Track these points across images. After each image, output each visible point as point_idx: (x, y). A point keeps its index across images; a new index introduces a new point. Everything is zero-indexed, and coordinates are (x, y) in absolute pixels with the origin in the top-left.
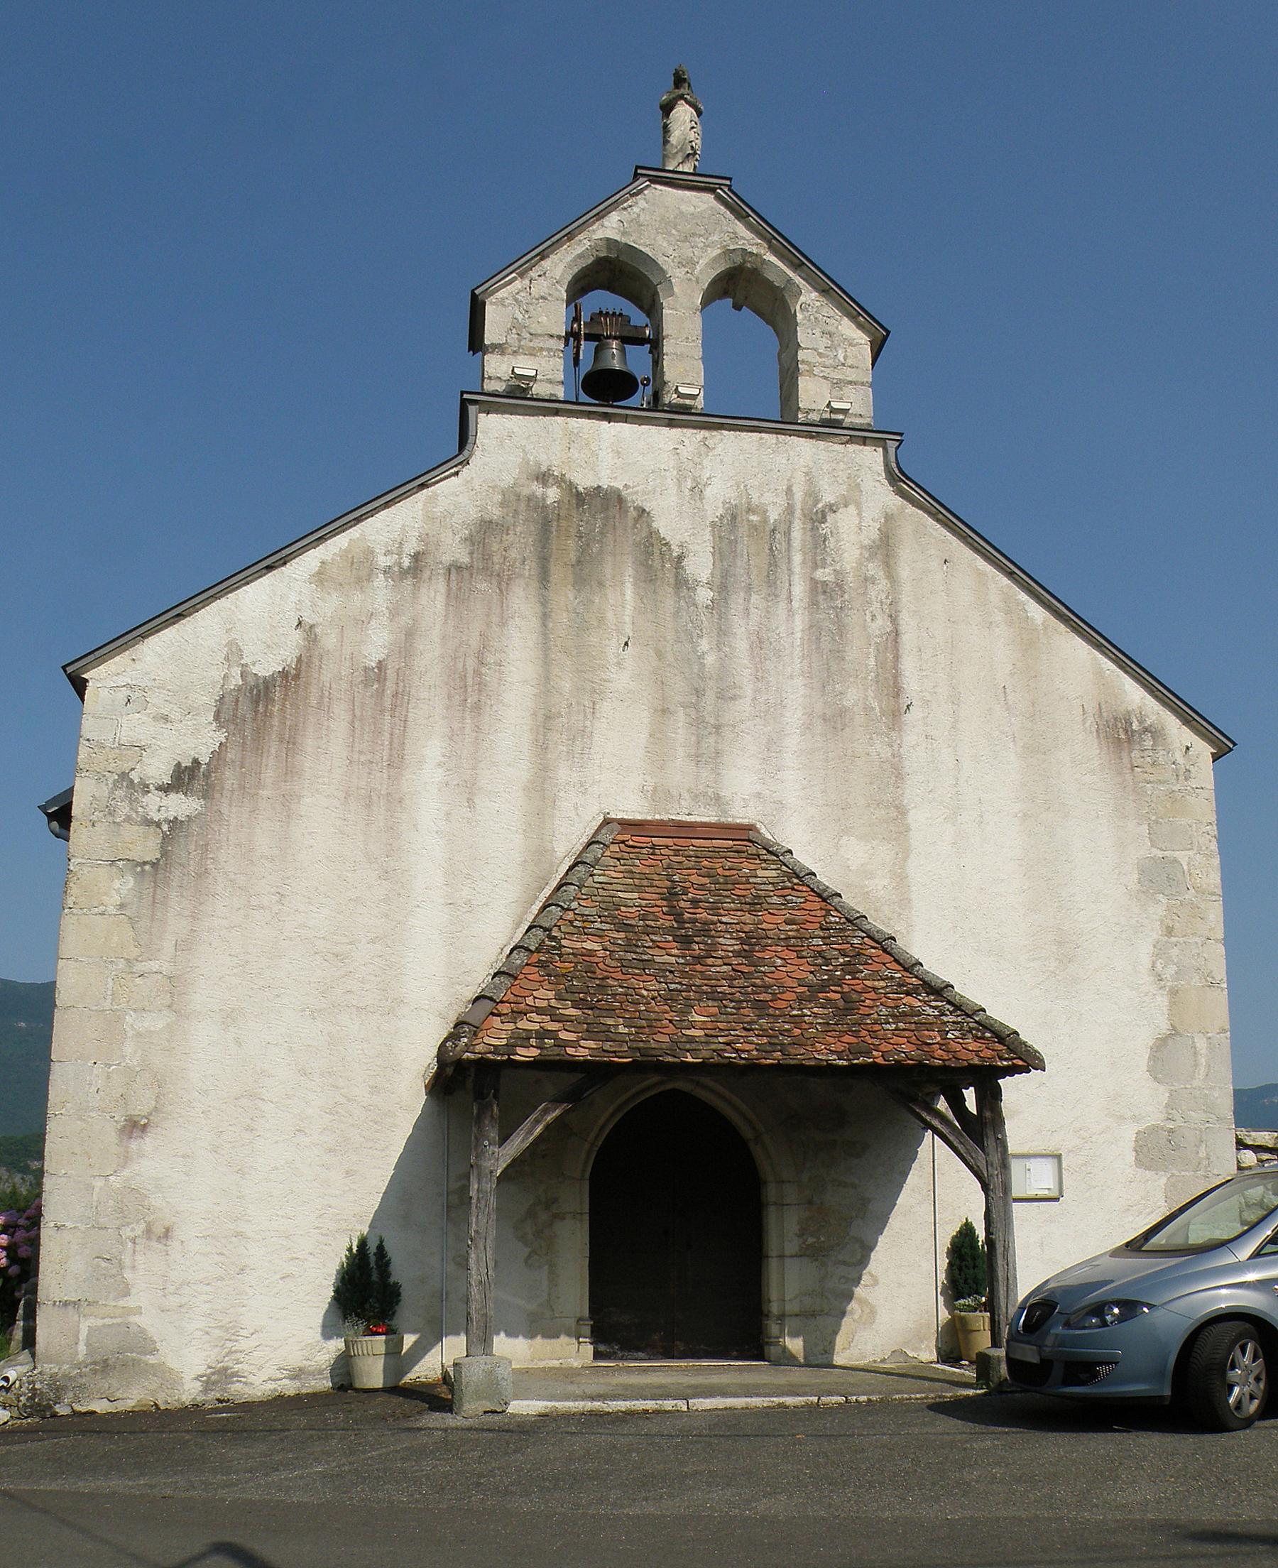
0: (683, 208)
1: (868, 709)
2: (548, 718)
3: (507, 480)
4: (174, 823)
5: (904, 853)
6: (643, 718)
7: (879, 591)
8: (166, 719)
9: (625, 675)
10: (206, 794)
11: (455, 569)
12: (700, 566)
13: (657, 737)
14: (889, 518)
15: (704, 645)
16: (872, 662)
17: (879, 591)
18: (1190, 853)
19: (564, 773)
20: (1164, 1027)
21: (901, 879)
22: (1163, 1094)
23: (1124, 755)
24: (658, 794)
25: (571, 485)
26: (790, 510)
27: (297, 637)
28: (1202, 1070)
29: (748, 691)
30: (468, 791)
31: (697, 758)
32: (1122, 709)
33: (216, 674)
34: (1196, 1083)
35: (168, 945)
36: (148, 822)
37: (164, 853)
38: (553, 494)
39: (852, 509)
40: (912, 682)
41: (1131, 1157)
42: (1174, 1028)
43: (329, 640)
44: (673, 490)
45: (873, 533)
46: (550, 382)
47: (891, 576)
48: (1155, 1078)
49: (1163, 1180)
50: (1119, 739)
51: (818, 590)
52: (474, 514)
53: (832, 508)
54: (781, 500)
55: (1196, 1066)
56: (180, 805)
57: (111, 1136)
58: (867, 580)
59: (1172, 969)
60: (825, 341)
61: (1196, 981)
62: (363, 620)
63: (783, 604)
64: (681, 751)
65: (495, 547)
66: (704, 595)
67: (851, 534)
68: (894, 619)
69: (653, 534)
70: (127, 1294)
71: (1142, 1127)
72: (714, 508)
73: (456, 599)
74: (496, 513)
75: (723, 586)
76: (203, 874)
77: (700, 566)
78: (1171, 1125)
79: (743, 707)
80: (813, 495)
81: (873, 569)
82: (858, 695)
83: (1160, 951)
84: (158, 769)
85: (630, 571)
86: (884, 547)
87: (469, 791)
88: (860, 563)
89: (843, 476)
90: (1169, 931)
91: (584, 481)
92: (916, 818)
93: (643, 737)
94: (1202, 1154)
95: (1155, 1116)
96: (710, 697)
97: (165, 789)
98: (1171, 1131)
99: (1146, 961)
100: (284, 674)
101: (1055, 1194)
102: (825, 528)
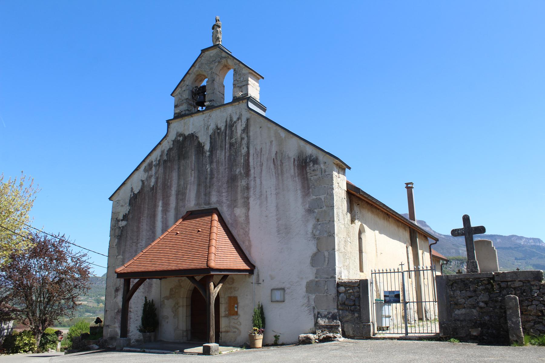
0: (211, 55)
1: (241, 174)
2: (179, 192)
3: (173, 138)
4: (123, 227)
5: (249, 209)
6: (195, 187)
7: (245, 142)
8: (122, 206)
9: (192, 177)
10: (127, 220)
11: (165, 161)
12: (207, 147)
13: (198, 192)
14: (248, 120)
15: (208, 166)
16: (242, 161)
17: (245, 142)
18: (325, 195)
19: (181, 204)
20: (314, 250)
21: (247, 217)
22: (314, 270)
23: (304, 170)
24: (198, 204)
25: (185, 135)
26: (226, 126)
27: (141, 184)
28: (327, 262)
29: (216, 175)
30: (165, 211)
31: (205, 195)
32: (304, 157)
33: (129, 195)
34: (325, 266)
35: (122, 253)
36: (120, 228)
37: (122, 233)
38: (181, 139)
39: (240, 121)
40: (251, 164)
41: (305, 289)
42: (318, 250)
43: (146, 183)
44: (203, 129)
45: (244, 126)
46: (185, 111)
47: (248, 137)
48: (312, 266)
49: (314, 297)
50: (303, 166)
51: (231, 145)
52: (168, 148)
53: (235, 122)
54: (224, 124)
55: (325, 261)
56: (124, 223)
57: (113, 292)
58: (242, 139)
59: (318, 232)
60: (239, 77)
61: (326, 235)
62: (150, 177)
63: (224, 151)
64: (202, 194)
65: (171, 154)
66: (208, 154)
67: (240, 127)
68: (248, 148)
69: (199, 142)
70: (115, 324)
71: (308, 280)
72: (211, 132)
73: (165, 168)
74: (172, 146)
75: (212, 150)
76: (127, 236)
77: (207, 147)
78: (317, 280)
79: (215, 179)
80: (231, 120)
81: (244, 136)
82: (239, 170)
83: (315, 227)
84: (121, 217)
85: (194, 153)
86: (246, 130)
87: (165, 211)
88: (241, 135)
89: (238, 113)
90: (318, 220)
91: (187, 133)
92: (251, 201)
93: (195, 192)
94: (326, 288)
95: (311, 277)
96: (208, 180)
97: (122, 220)
98: (317, 281)
99: (311, 231)
100: (139, 192)
101: (282, 300)
102: (234, 128)
